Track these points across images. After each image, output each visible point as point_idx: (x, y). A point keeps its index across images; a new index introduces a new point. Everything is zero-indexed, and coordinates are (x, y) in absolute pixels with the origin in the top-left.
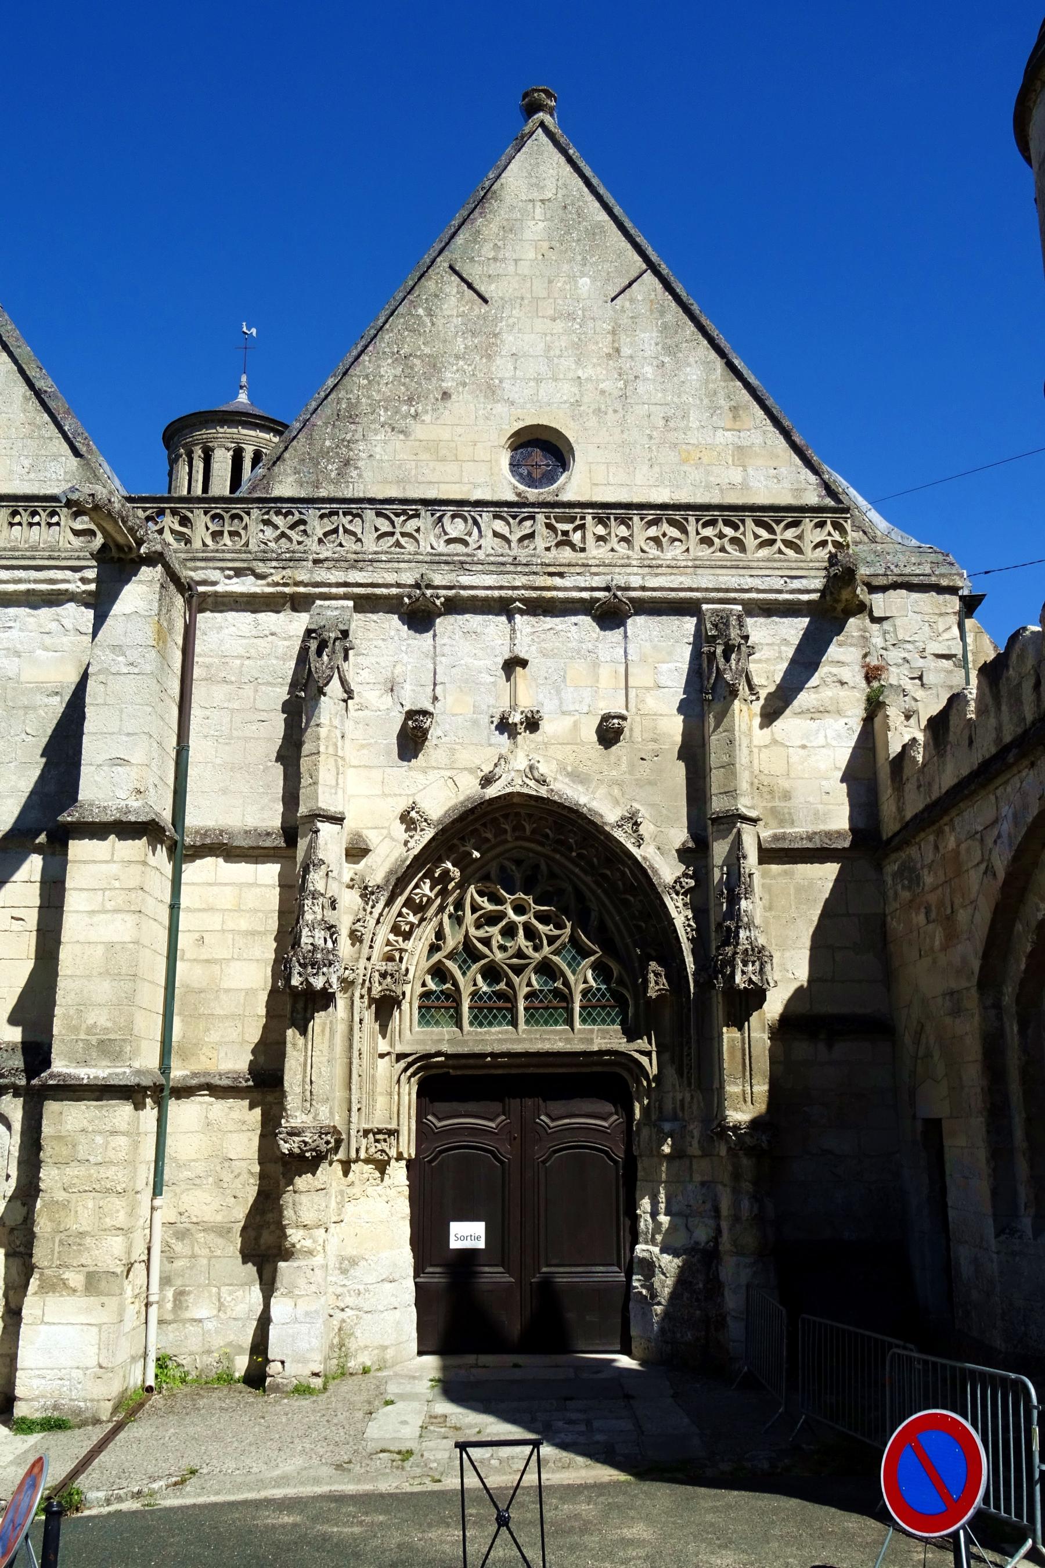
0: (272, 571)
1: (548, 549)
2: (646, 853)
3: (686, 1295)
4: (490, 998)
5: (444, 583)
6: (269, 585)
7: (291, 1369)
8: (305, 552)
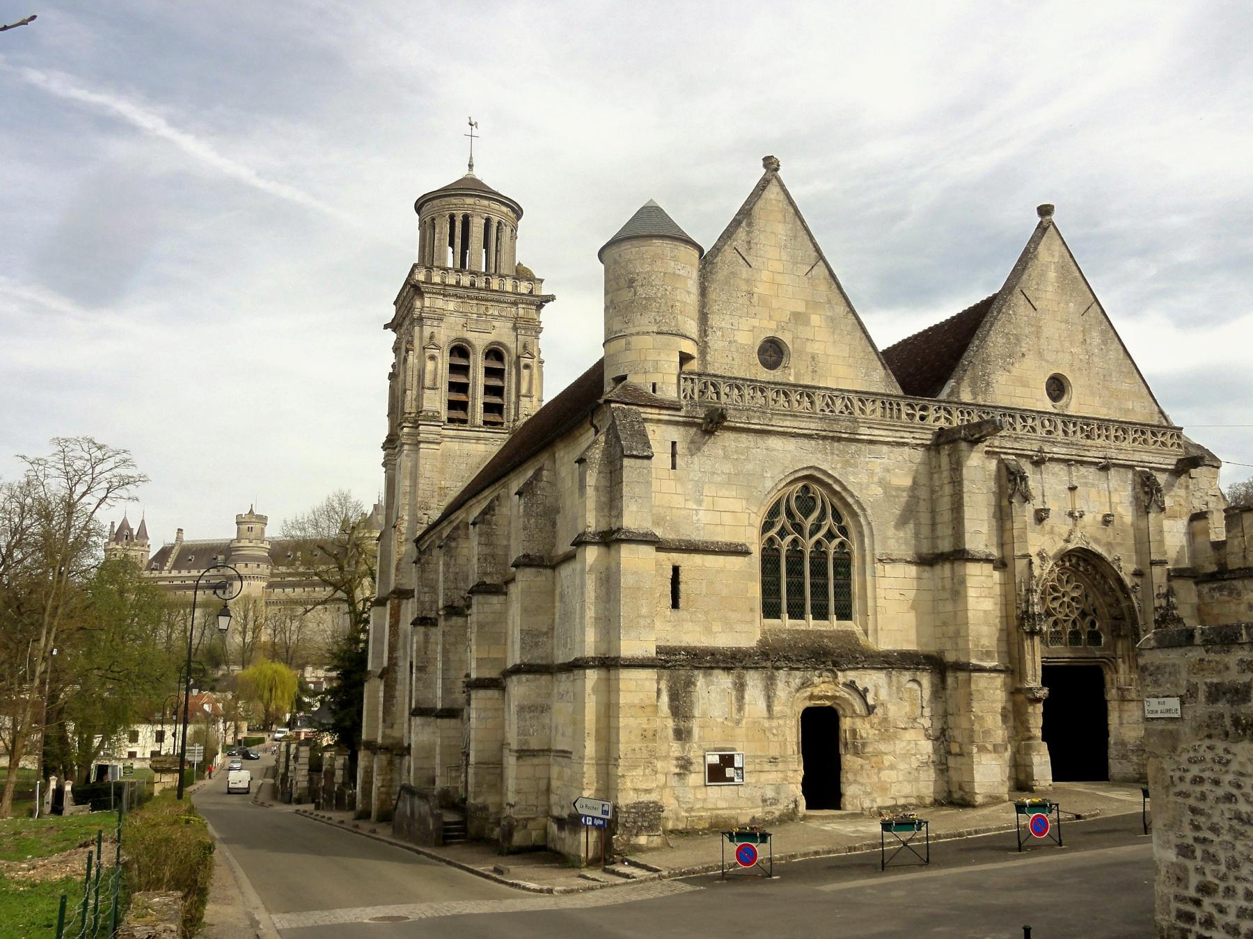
2: (1122, 574)
7: (1042, 783)
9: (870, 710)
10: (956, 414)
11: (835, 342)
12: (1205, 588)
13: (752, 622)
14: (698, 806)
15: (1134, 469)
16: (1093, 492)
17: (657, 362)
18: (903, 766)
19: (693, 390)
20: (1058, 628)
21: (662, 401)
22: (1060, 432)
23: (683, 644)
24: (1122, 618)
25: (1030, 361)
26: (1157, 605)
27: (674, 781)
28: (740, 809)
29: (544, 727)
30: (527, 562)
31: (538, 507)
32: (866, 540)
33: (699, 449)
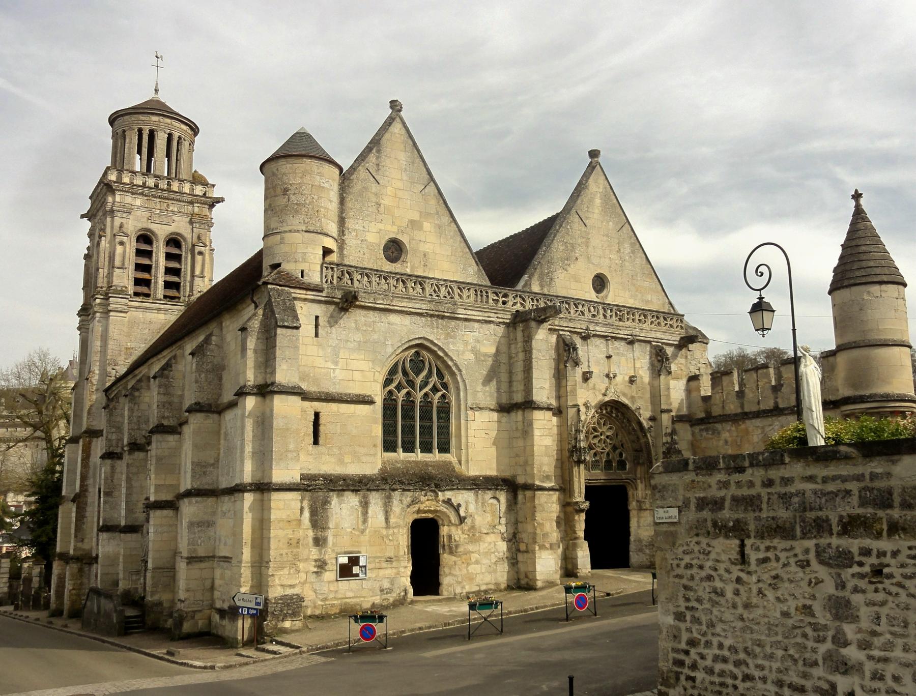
2: (641, 419)
7: (584, 571)
9: (462, 520)
10: (528, 300)
11: (441, 244)
12: (697, 429)
13: (375, 455)
14: (331, 596)
16: (623, 359)
17: (305, 254)
18: (485, 561)
19: (332, 277)
20: (597, 458)
21: (308, 284)
22: (601, 316)
23: (322, 472)
24: (641, 451)
25: (581, 264)
26: (664, 441)
27: (312, 578)
28: (364, 597)
29: (209, 538)
30: (197, 408)
31: (208, 365)
32: (462, 394)
33: (336, 322)
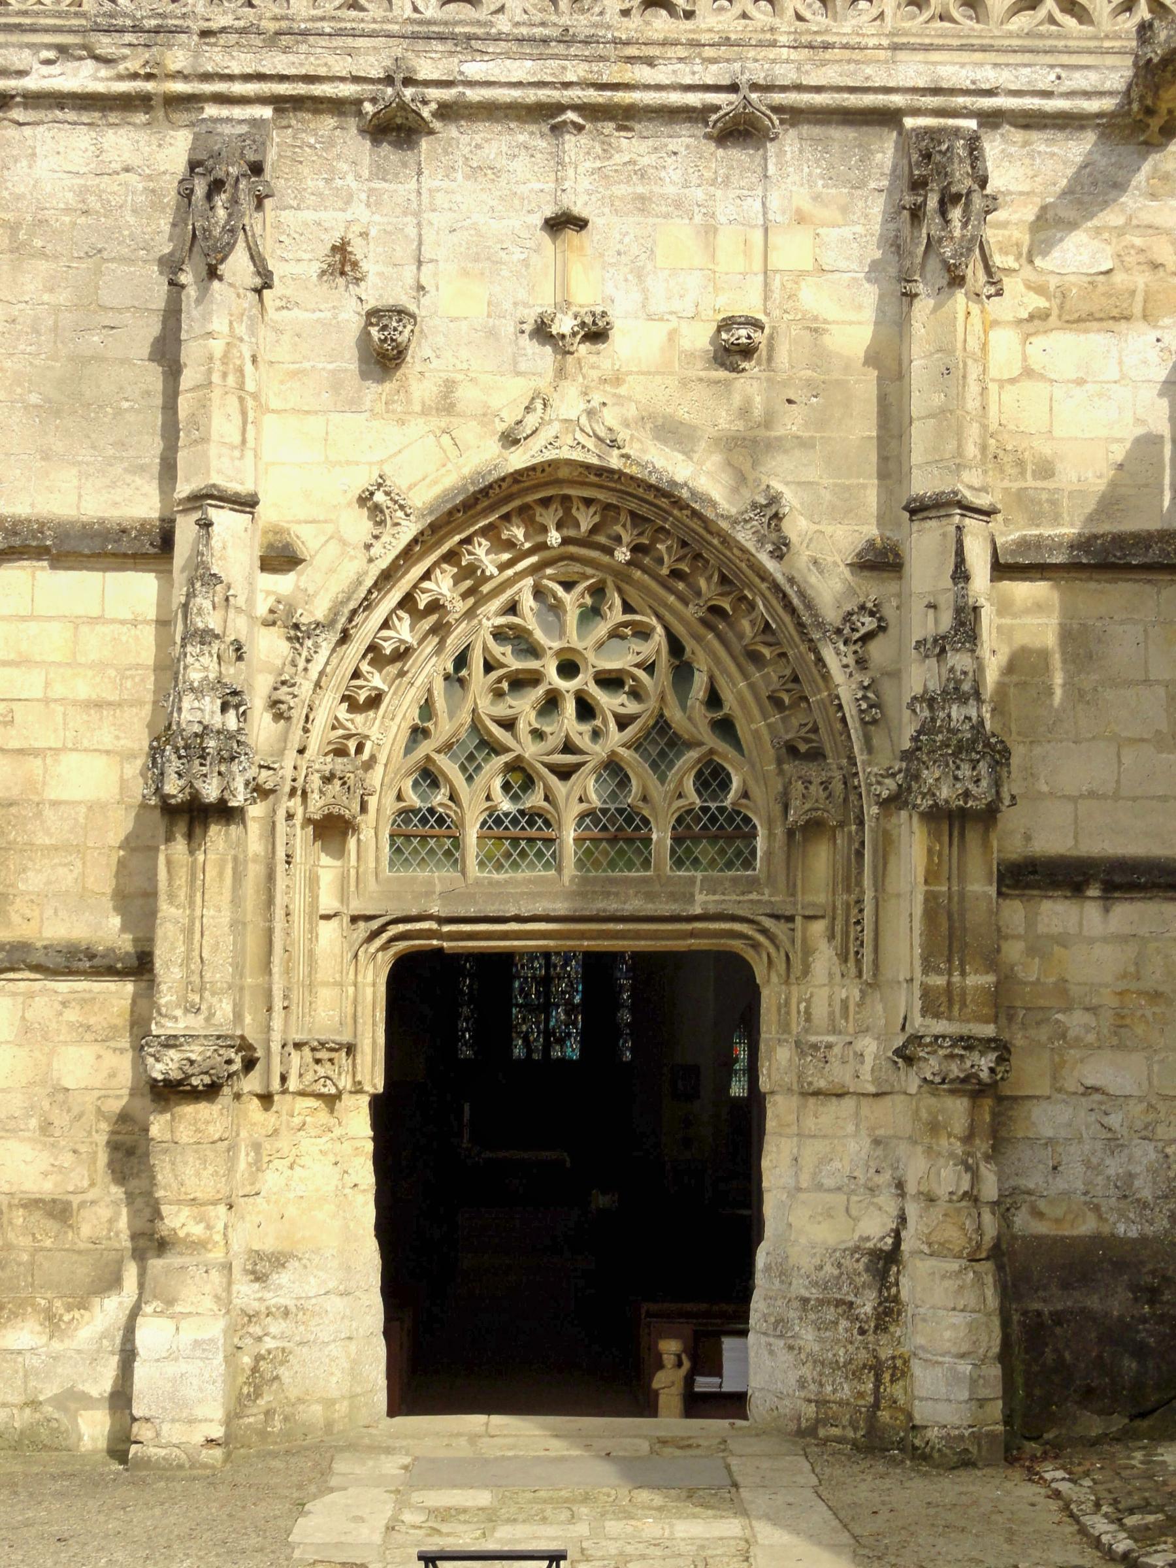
0: (126, 51)
1: (626, 13)
3: (844, 1323)
4: (515, 822)
5: (435, 76)
6: (120, 78)
7: (172, 1432)
8: (184, 16)
15: (899, 125)
